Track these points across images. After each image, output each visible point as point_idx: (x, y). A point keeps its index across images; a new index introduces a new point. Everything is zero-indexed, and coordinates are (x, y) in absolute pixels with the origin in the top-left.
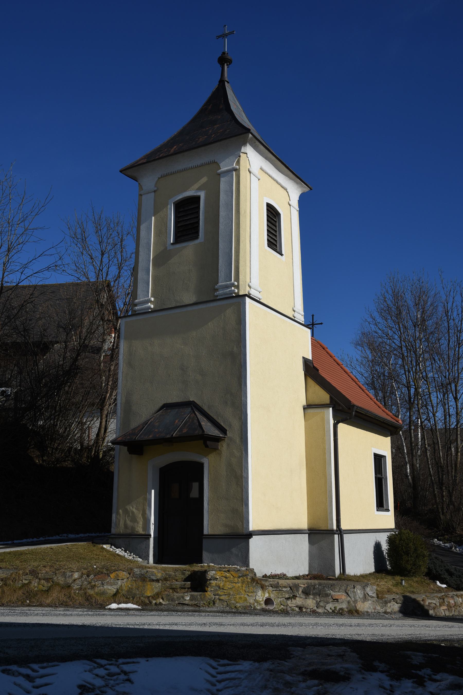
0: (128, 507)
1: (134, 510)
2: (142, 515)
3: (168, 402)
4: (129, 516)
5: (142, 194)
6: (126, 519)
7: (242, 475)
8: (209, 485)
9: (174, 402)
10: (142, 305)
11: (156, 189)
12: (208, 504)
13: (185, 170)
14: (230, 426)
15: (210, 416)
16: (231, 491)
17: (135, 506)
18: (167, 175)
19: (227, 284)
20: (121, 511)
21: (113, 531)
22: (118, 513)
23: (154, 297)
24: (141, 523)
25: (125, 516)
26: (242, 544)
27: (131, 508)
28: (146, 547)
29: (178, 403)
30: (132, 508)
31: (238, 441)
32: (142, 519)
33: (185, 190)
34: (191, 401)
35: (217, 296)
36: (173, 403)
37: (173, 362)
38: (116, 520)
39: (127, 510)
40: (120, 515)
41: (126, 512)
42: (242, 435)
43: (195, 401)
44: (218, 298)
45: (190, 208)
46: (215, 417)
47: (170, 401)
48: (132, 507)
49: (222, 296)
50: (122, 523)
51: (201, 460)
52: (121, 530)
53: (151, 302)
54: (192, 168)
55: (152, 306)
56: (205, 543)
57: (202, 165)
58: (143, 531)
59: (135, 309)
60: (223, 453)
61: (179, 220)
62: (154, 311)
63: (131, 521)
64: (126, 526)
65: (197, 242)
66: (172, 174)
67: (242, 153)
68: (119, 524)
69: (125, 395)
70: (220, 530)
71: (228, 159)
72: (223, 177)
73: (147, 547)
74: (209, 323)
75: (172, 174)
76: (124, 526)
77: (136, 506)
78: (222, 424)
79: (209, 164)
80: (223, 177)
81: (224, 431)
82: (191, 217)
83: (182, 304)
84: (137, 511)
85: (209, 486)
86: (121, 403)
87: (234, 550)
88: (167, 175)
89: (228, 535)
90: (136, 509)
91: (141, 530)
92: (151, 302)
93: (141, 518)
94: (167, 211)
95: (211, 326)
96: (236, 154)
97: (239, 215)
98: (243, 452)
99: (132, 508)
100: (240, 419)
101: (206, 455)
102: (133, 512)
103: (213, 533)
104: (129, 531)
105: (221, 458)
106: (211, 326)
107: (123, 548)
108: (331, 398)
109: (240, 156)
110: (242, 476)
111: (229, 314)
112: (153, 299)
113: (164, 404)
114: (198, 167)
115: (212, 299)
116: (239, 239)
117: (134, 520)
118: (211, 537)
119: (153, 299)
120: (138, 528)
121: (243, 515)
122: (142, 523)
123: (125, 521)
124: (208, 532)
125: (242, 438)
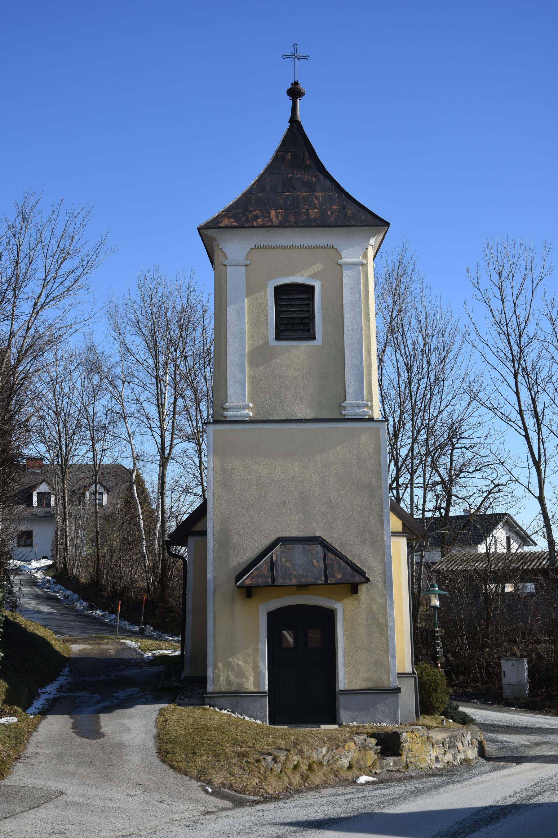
0: (230, 660)
1: (241, 663)
2: (252, 669)
3: (284, 536)
4: (233, 670)
5: (227, 265)
6: (228, 674)
7: (387, 624)
8: (344, 634)
9: (292, 536)
10: (237, 410)
11: (248, 262)
12: (344, 656)
13: (291, 247)
14: (370, 568)
15: (344, 556)
16: (374, 641)
17: (241, 658)
18: (264, 247)
19: (359, 403)
20: (220, 664)
21: (210, 688)
22: (215, 667)
23: (252, 403)
24: (252, 678)
25: (228, 671)
26: (390, 699)
27: (236, 660)
28: (262, 707)
29: (298, 537)
30: (239, 661)
31: (380, 585)
32: (252, 673)
33: (292, 274)
34: (316, 537)
35: (345, 415)
36: (291, 537)
37: (289, 488)
38: (213, 675)
39: (230, 663)
40: (219, 669)
41: (229, 666)
42: (385, 579)
43: (322, 536)
44: (346, 417)
45: (298, 297)
46: (350, 558)
47: (286, 534)
48: (238, 660)
49: (351, 415)
50: (223, 679)
51: (333, 606)
52: (223, 686)
53: (249, 408)
54: (300, 247)
55: (251, 414)
56: (342, 700)
57: (315, 247)
58: (255, 687)
59: (227, 414)
60: (362, 598)
61: (282, 310)
62: (253, 422)
63: (236, 677)
64: (229, 682)
65: (311, 343)
66: (271, 247)
67: (370, 245)
68: (219, 681)
69: (218, 522)
70: (359, 684)
71: (351, 248)
72: (346, 270)
73: (263, 706)
74: (338, 447)
75: (271, 247)
76: (227, 682)
77: (244, 658)
78: (359, 566)
79: (325, 247)
80: (346, 270)
81: (362, 573)
82: (298, 310)
83: (295, 418)
84: (245, 664)
85: (344, 636)
86: (213, 532)
87: (379, 706)
88: (264, 247)
89: (370, 690)
90: (243, 662)
91: (252, 686)
92: (249, 408)
93: (252, 672)
94: (266, 295)
95: (341, 451)
96: (363, 244)
97: (369, 322)
98: (388, 599)
99: (239, 661)
100: (383, 561)
101: (340, 600)
102: (239, 666)
103: (351, 688)
104: (233, 689)
105: (359, 604)
106: (341, 451)
107: (229, 709)
108: (403, 524)
109: (367, 249)
110: (386, 625)
111: (365, 439)
112: (251, 405)
113: (279, 538)
114: (310, 248)
115: (336, 417)
116: (371, 351)
117: (241, 674)
118: (347, 692)
119: (251, 405)
120: (248, 685)
121: (389, 668)
122: (254, 679)
123: (228, 676)
124: (345, 686)
125: (385, 583)
